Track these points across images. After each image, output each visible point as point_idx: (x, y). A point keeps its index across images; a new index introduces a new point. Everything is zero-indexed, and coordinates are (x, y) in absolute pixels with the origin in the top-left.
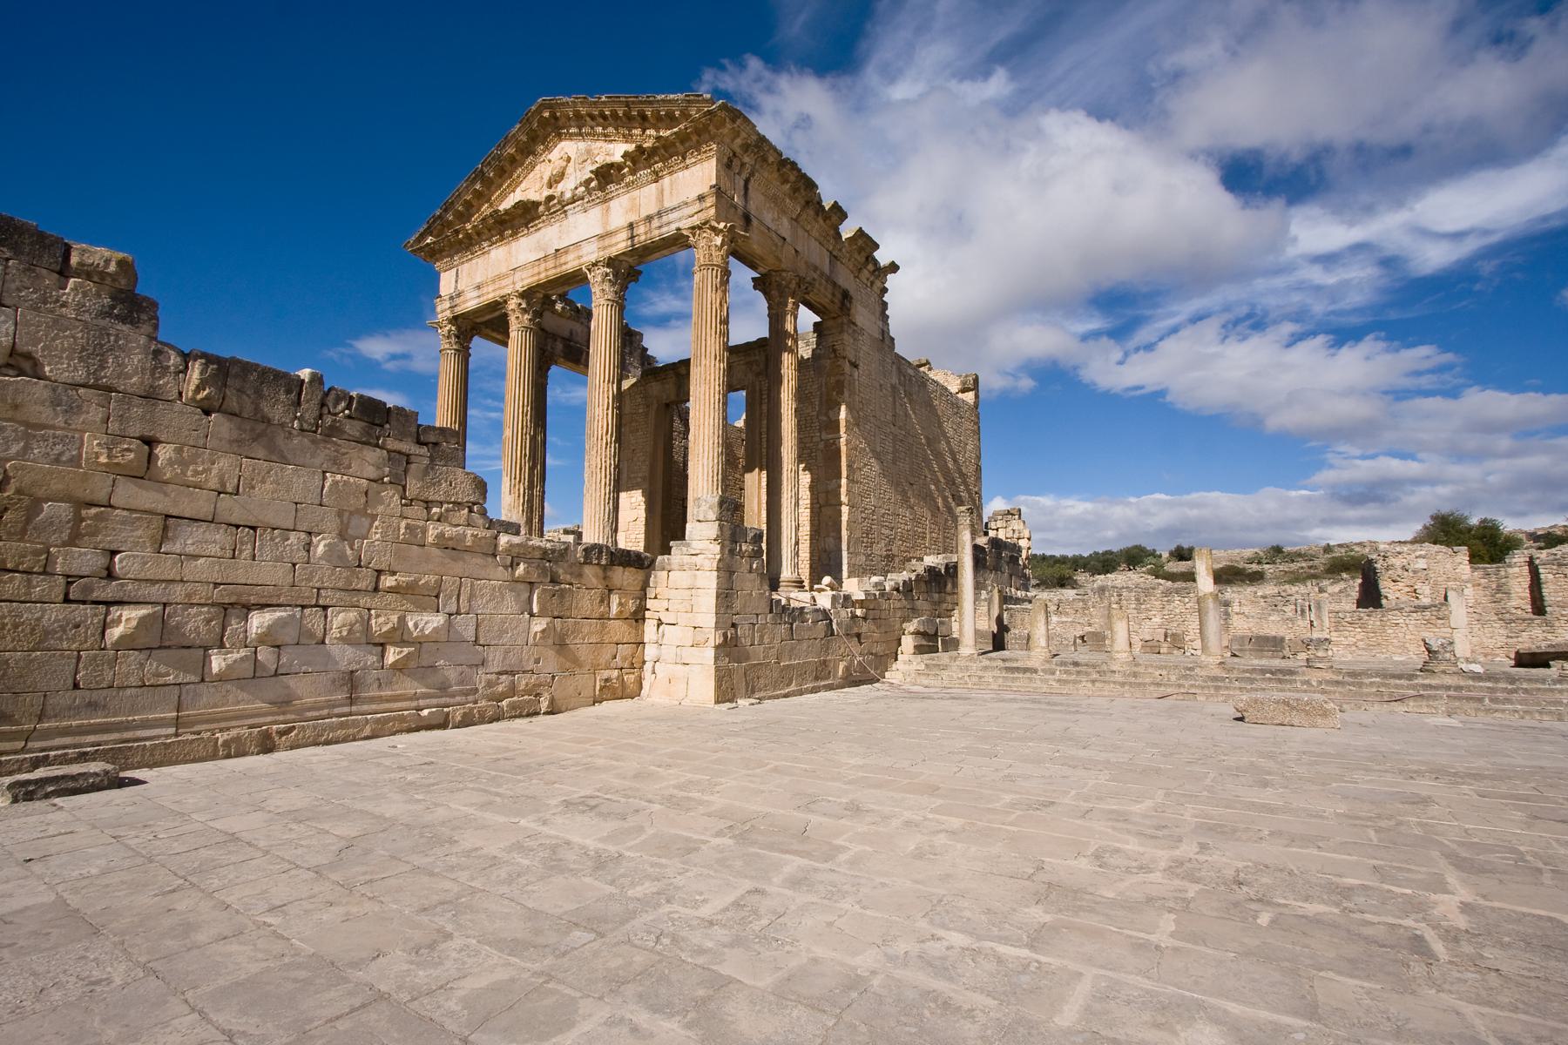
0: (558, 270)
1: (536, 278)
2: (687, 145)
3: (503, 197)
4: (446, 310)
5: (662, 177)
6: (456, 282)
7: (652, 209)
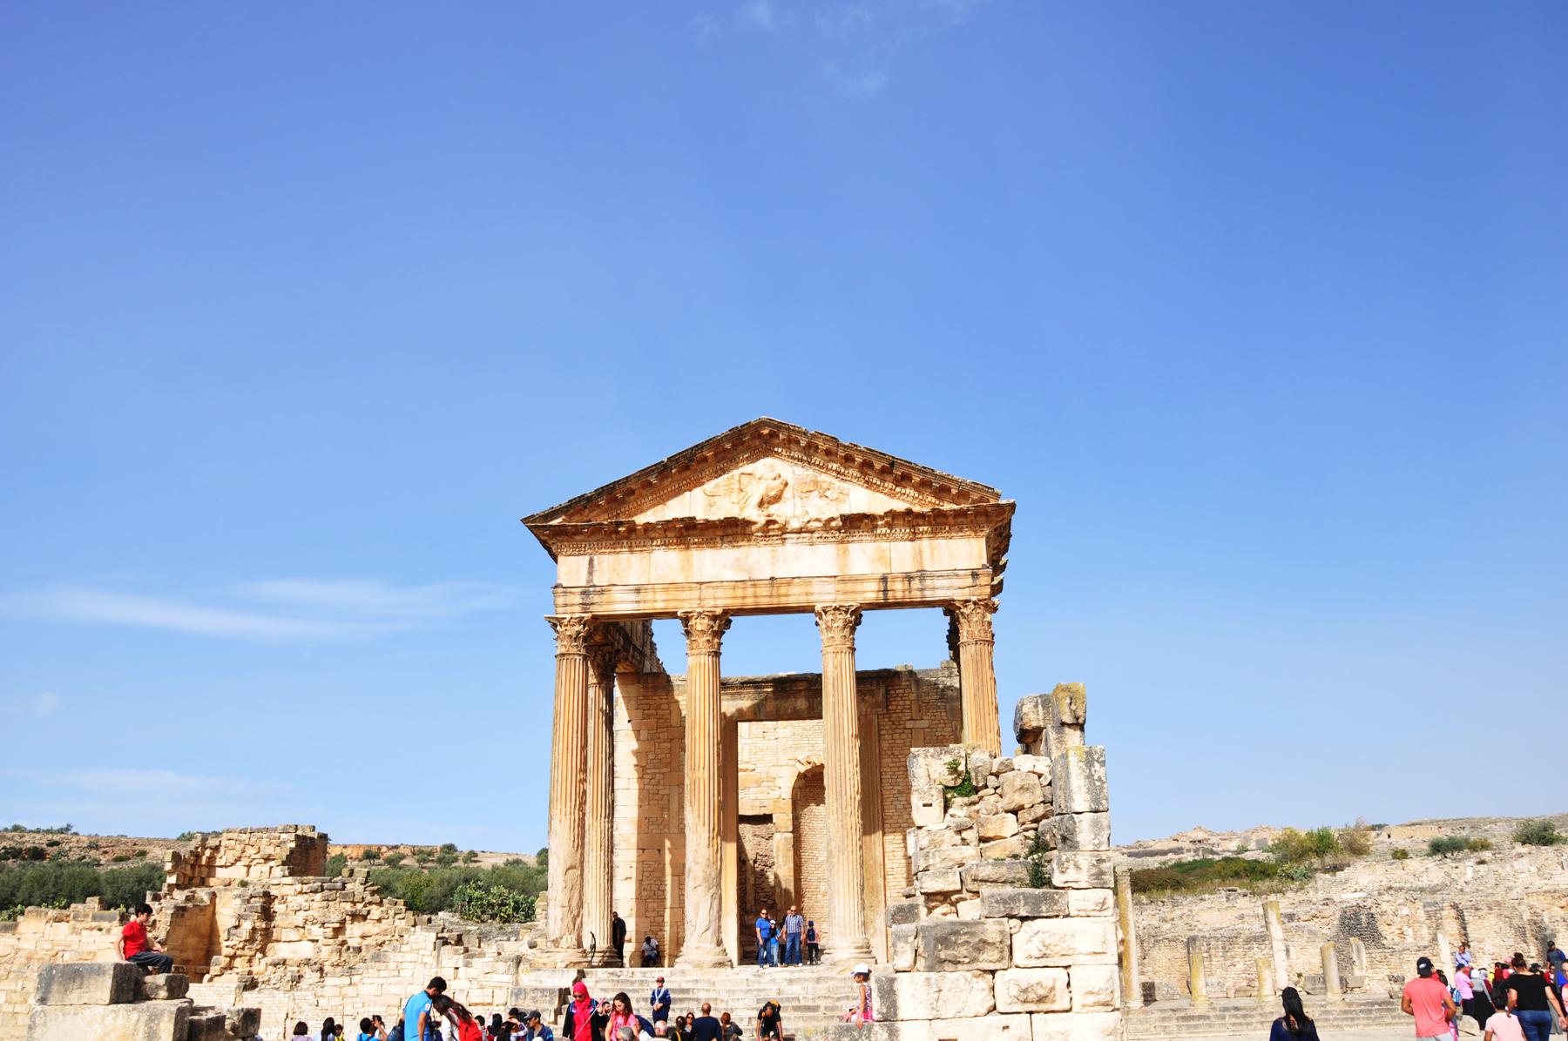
2: (960, 520)
3: (677, 493)
4: (572, 605)
5: (920, 539)
6: (590, 573)
7: (910, 567)
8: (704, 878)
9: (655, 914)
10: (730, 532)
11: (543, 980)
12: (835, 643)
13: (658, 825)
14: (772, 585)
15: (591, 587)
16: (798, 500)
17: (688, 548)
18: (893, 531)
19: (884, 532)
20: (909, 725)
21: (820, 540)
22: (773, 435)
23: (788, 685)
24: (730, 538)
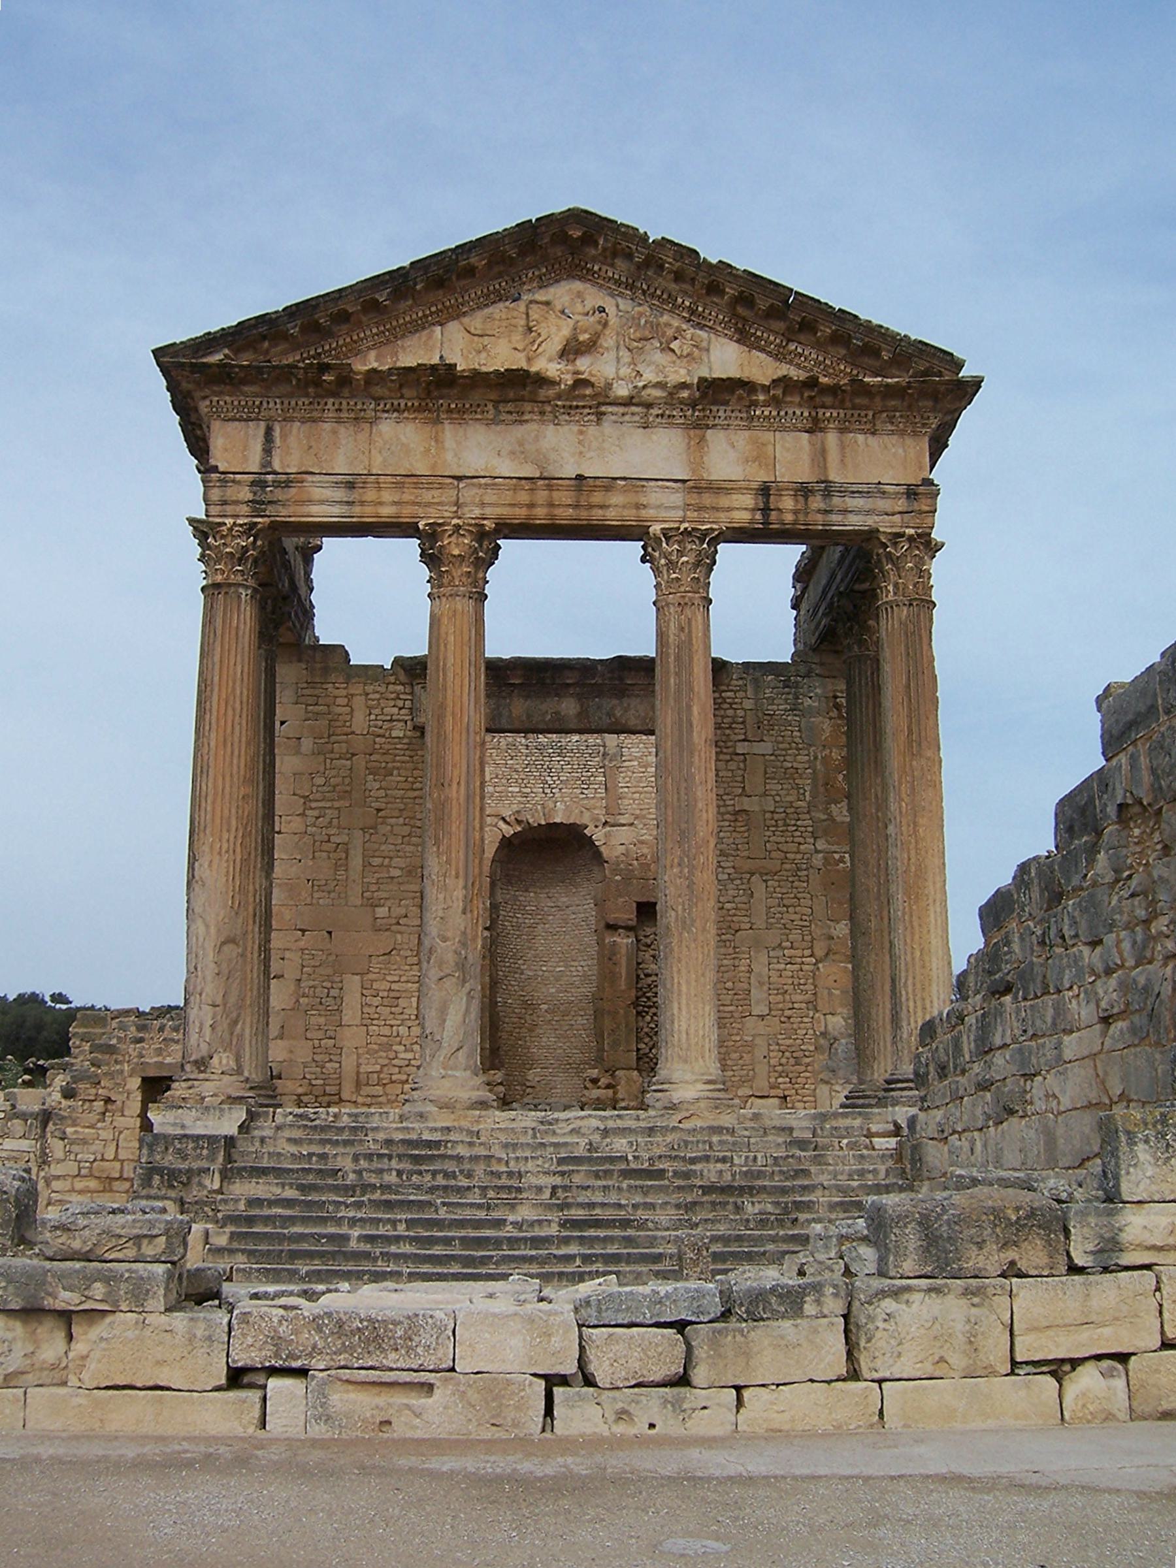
0: (584, 514)
1: (522, 512)
3: (419, 326)
4: (236, 502)
5: (822, 430)
7: (804, 473)
8: (457, 964)
9: (320, 1034)
10: (511, 395)
11: (188, 1123)
12: (682, 589)
13: (329, 892)
14: (579, 490)
15: (269, 473)
16: (624, 353)
17: (437, 421)
18: (782, 413)
19: (767, 413)
20: (741, 748)
21: (659, 420)
22: (588, 240)
23: (548, 674)
24: (510, 407)
